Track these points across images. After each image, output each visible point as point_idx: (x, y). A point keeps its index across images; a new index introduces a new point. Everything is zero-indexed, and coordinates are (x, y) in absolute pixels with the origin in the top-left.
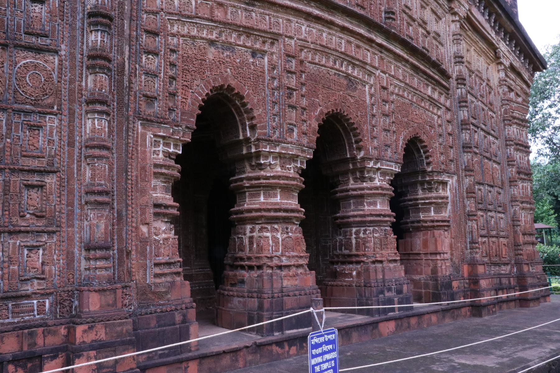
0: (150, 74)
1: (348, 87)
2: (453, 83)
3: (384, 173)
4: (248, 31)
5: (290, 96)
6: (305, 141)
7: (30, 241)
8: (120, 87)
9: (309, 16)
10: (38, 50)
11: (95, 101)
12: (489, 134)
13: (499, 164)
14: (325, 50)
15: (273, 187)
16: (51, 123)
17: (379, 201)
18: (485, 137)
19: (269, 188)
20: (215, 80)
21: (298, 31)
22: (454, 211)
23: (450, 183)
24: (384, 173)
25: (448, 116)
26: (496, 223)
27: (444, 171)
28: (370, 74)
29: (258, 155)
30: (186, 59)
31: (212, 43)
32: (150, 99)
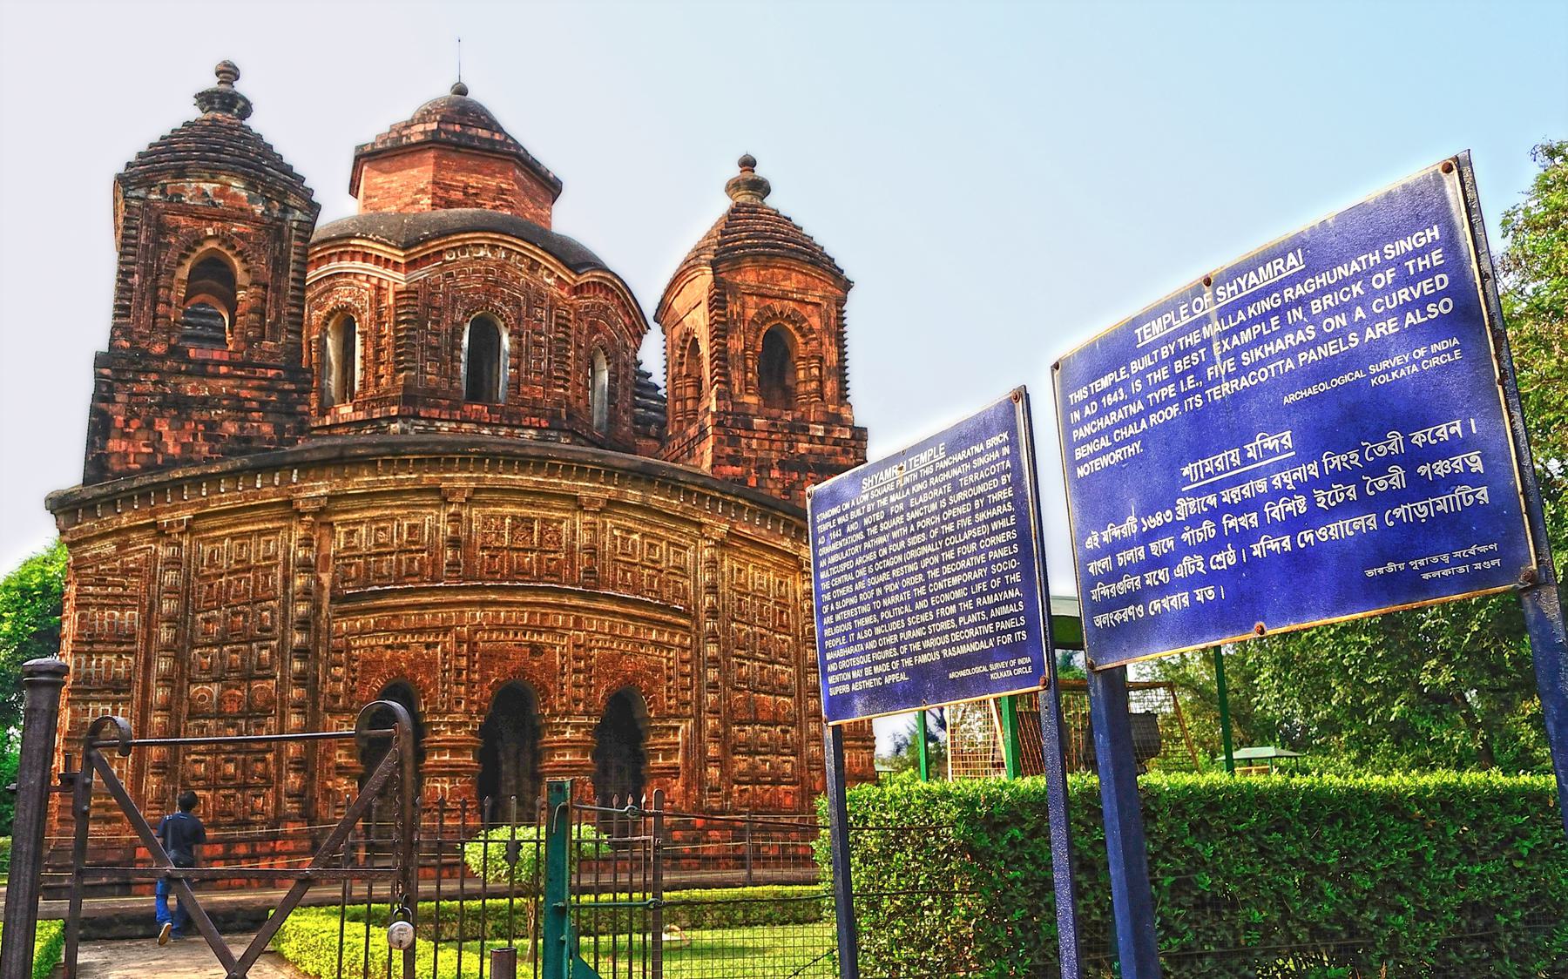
0: (337, 679)
1: (532, 653)
2: (702, 616)
3: (577, 727)
4: (421, 631)
5: (459, 674)
6: (475, 708)
7: (256, 792)
8: (314, 693)
9: (483, 604)
10: (264, 678)
11: (299, 706)
12: (772, 662)
13: (791, 696)
14: (504, 628)
15: (444, 748)
16: (271, 721)
17: (568, 752)
18: (762, 668)
19: (441, 750)
20: (391, 673)
21: (474, 617)
22: (686, 757)
23: (683, 727)
24: (577, 727)
25: (687, 655)
26: (771, 767)
27: (670, 716)
28: (563, 636)
29: (431, 724)
30: (365, 663)
31: (388, 647)
32: (336, 698)
